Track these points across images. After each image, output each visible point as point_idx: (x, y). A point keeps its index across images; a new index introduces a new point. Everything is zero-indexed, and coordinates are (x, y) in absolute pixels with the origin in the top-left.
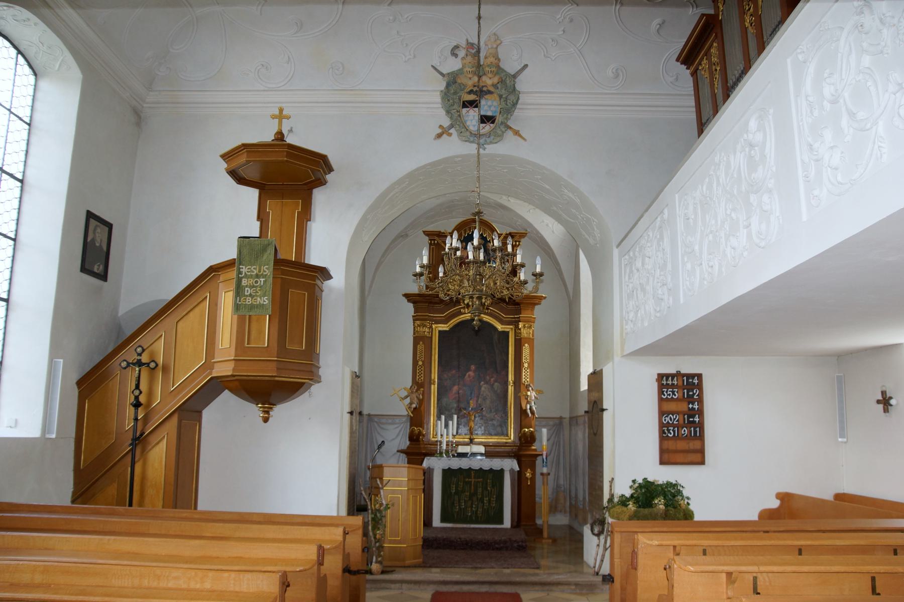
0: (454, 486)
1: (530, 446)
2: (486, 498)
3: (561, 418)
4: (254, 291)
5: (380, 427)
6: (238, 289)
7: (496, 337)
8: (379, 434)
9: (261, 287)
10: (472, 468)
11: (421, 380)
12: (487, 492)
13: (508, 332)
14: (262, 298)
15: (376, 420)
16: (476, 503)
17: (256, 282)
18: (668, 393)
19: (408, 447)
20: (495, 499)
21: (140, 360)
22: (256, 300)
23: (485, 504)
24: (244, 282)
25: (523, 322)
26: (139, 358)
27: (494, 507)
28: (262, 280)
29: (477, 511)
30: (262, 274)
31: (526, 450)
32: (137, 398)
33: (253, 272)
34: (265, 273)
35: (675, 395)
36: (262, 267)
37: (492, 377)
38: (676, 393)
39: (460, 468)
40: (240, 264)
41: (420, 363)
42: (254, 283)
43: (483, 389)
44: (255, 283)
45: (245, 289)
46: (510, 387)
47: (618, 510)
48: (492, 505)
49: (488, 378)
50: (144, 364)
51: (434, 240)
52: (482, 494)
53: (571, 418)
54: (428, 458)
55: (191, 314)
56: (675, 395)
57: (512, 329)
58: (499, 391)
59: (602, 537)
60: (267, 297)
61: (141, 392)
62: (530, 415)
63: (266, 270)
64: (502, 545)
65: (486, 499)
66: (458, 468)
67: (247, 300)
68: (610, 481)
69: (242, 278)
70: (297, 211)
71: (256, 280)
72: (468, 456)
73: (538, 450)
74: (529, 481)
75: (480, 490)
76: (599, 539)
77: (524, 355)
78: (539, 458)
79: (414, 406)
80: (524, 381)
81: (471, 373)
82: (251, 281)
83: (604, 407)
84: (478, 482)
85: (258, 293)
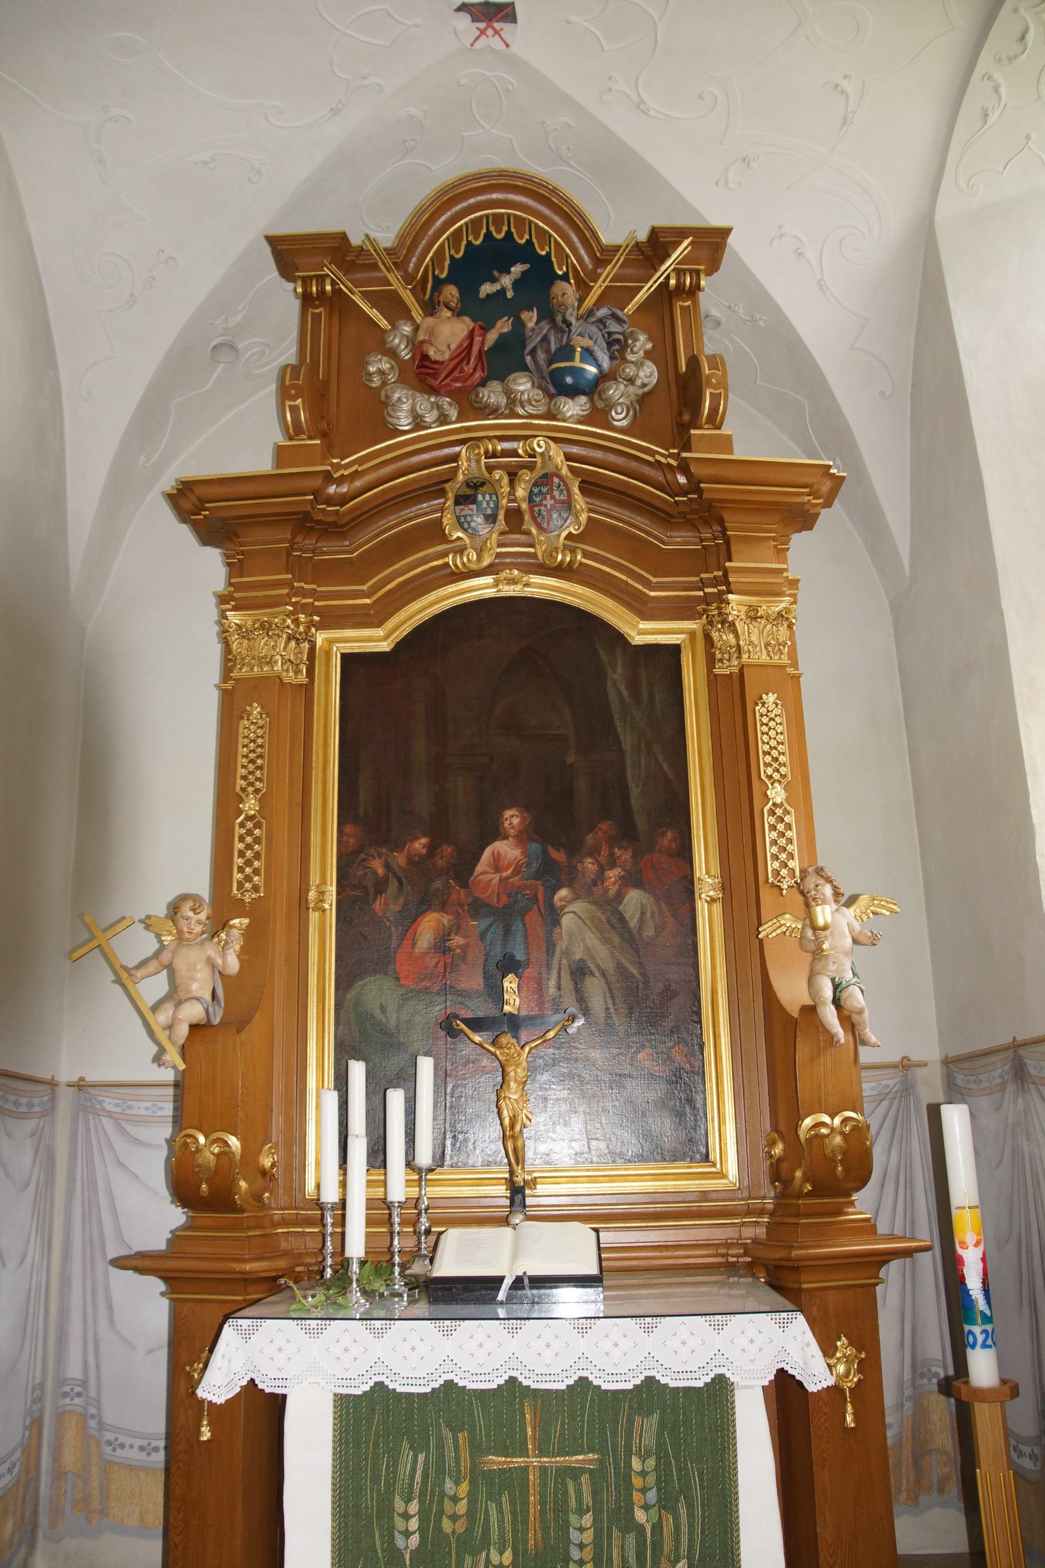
0: (414, 1507)
1: (841, 1213)
3: (905, 1065)
5: (124, 1133)
7: (617, 675)
8: (120, 1164)
11: (256, 888)
12: (631, 1539)
13: (676, 649)
15: (109, 1104)
19: (177, 1239)
37: (613, 864)
41: (250, 805)
43: (566, 921)
46: (702, 908)
51: (321, 279)
54: (245, 1323)
57: (692, 634)
58: (649, 932)
72: (502, 1295)
73: (882, 1229)
74: (849, 1408)
78: (893, 1270)
79: (193, 1012)
80: (777, 873)
81: (506, 849)
84: (575, 1473)
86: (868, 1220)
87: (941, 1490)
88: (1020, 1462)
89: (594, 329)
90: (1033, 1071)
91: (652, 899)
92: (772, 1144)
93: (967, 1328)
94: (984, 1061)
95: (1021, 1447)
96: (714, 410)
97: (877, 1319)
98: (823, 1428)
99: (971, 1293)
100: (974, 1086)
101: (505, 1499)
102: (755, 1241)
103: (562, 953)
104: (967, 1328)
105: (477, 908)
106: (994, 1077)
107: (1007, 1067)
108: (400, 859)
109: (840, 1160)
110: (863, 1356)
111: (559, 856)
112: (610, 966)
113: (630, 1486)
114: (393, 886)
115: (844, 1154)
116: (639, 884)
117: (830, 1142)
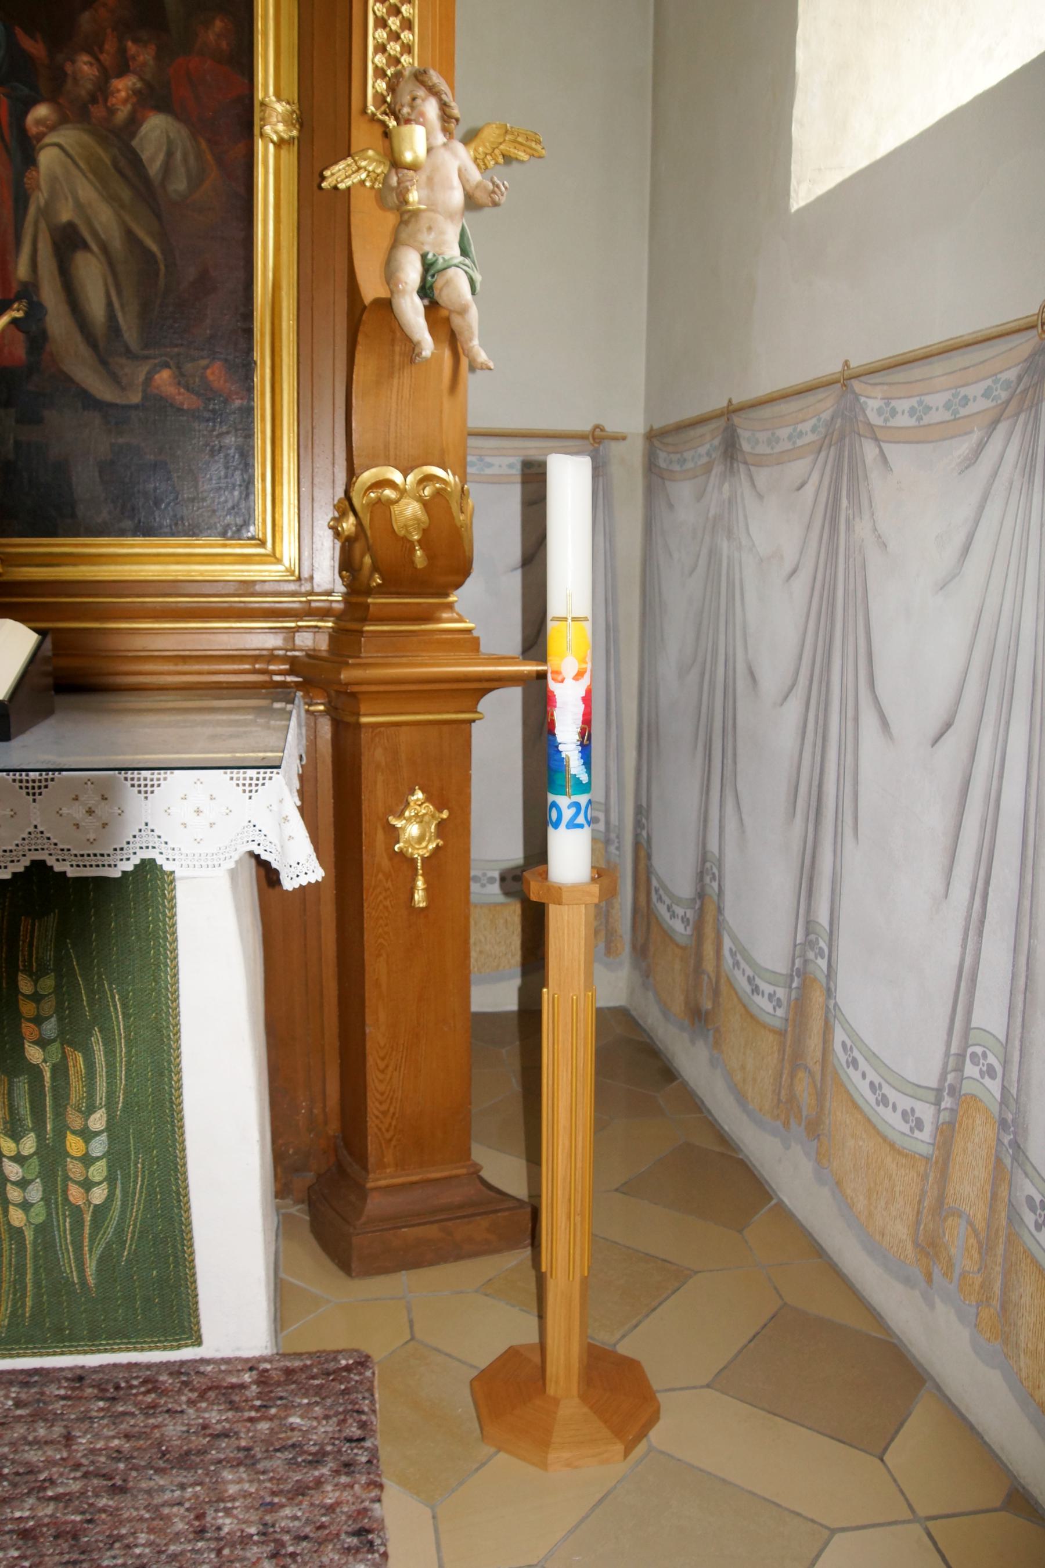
1: (428, 616)
20: (98, 1147)
27: (100, 1212)
31: (397, 644)
37: (123, 68)
43: (47, 158)
46: (266, 155)
49: (85, 67)
53: (655, 437)
58: (179, 185)
62: (427, 343)
74: (420, 883)
86: (469, 631)
88: (671, 922)
90: (746, 447)
91: (185, 132)
92: (342, 516)
93: (551, 798)
94: (692, 433)
95: (675, 908)
97: (469, 768)
98: (381, 907)
99: (561, 748)
100: (677, 468)
102: (312, 655)
103: (39, 209)
104: (551, 798)
106: (700, 456)
107: (716, 442)
109: (419, 541)
110: (445, 815)
111: (34, 47)
115: (425, 532)
116: (164, 106)
117: (401, 512)
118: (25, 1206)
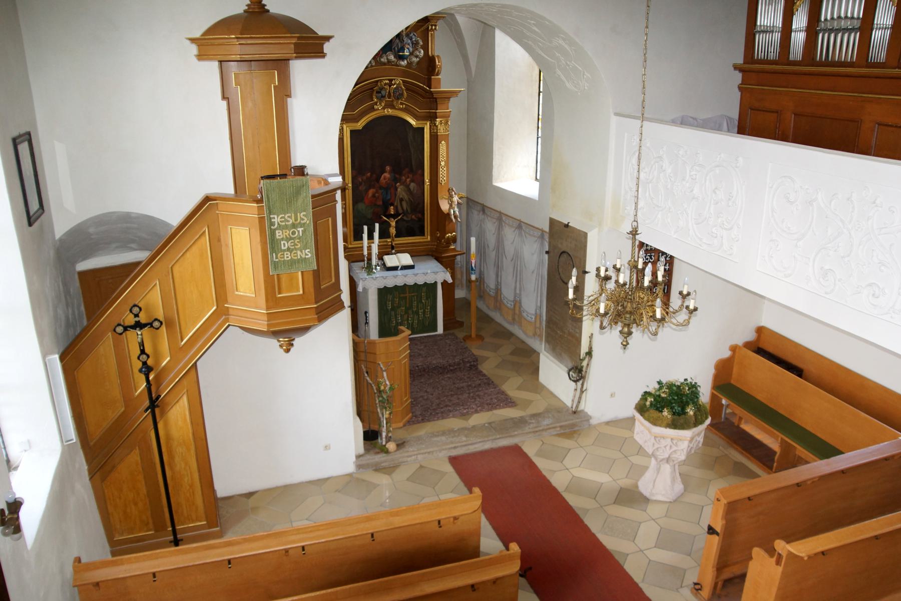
0: (390, 303)
2: (421, 310)
4: (292, 244)
6: (272, 245)
9: (298, 239)
10: (407, 284)
12: (422, 304)
14: (303, 251)
16: (412, 316)
17: (294, 233)
18: (647, 257)
20: (429, 310)
21: (139, 321)
22: (295, 255)
23: (420, 316)
24: (279, 234)
25: (440, 118)
26: (137, 319)
27: (428, 317)
28: (300, 230)
29: (413, 323)
30: (300, 223)
32: (145, 363)
33: (288, 221)
34: (302, 222)
35: (652, 259)
36: (299, 214)
37: (408, 178)
38: (653, 257)
39: (396, 285)
40: (270, 213)
42: (291, 234)
43: (399, 190)
44: (292, 234)
45: (280, 243)
47: (653, 415)
48: (426, 316)
50: (145, 325)
52: (417, 307)
55: (188, 254)
56: (652, 259)
58: (415, 191)
59: (579, 383)
60: (309, 250)
61: (148, 356)
62: (454, 220)
63: (304, 217)
64: (456, 367)
65: (421, 311)
66: (394, 285)
67: (285, 256)
68: (590, 337)
69: (275, 230)
70: (272, 85)
71: (294, 230)
75: (415, 304)
76: (576, 384)
77: (441, 154)
81: (387, 175)
82: (288, 233)
83: (587, 270)
84: (414, 296)
85: (297, 245)
87: (458, 286)
89: (409, 41)
96: (438, 71)
101: (404, 301)
105: (381, 188)
108: (365, 178)
111: (397, 176)
112: (407, 200)
113: (422, 297)
114: (363, 184)
118: (421, 317)
